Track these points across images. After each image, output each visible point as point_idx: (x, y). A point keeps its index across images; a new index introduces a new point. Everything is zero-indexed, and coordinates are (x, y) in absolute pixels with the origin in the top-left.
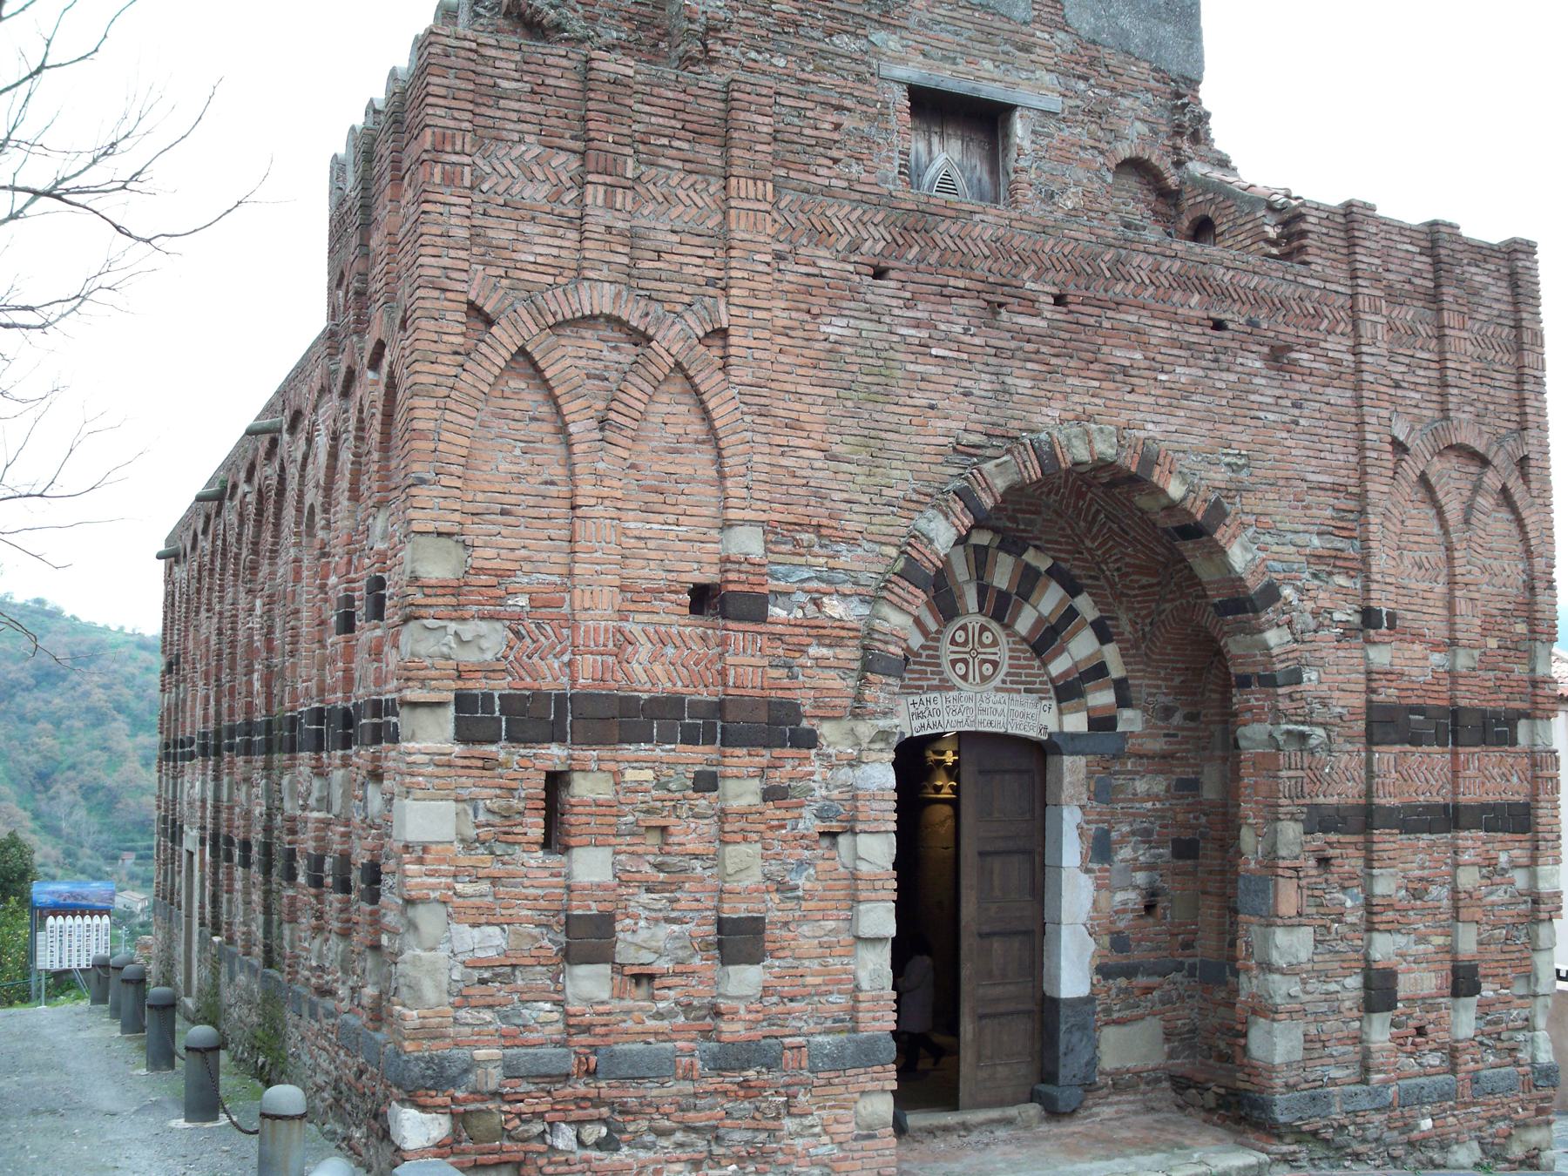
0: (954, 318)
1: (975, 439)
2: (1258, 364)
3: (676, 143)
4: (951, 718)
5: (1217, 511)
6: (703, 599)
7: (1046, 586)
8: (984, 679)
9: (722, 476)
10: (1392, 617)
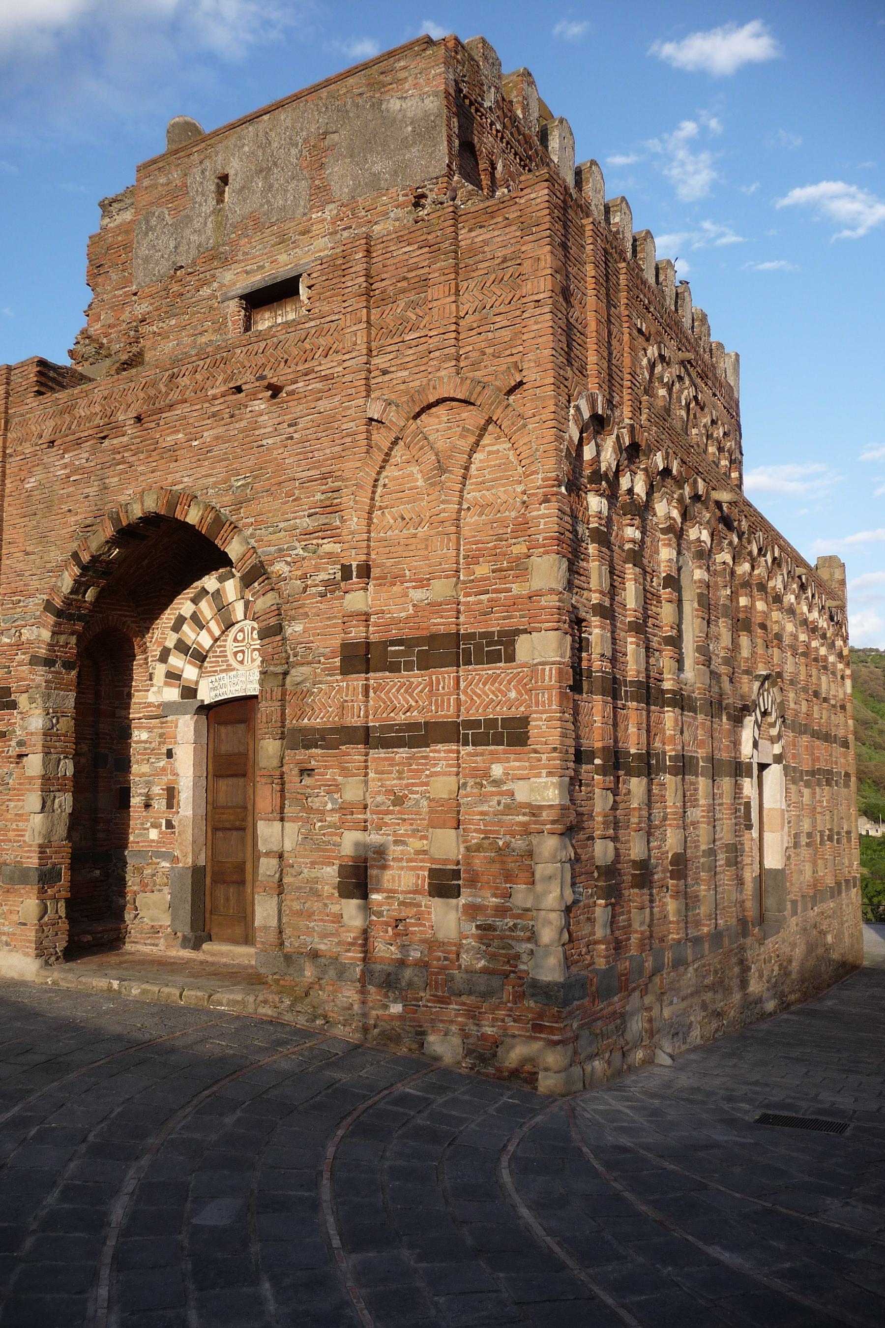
4: (233, 689)
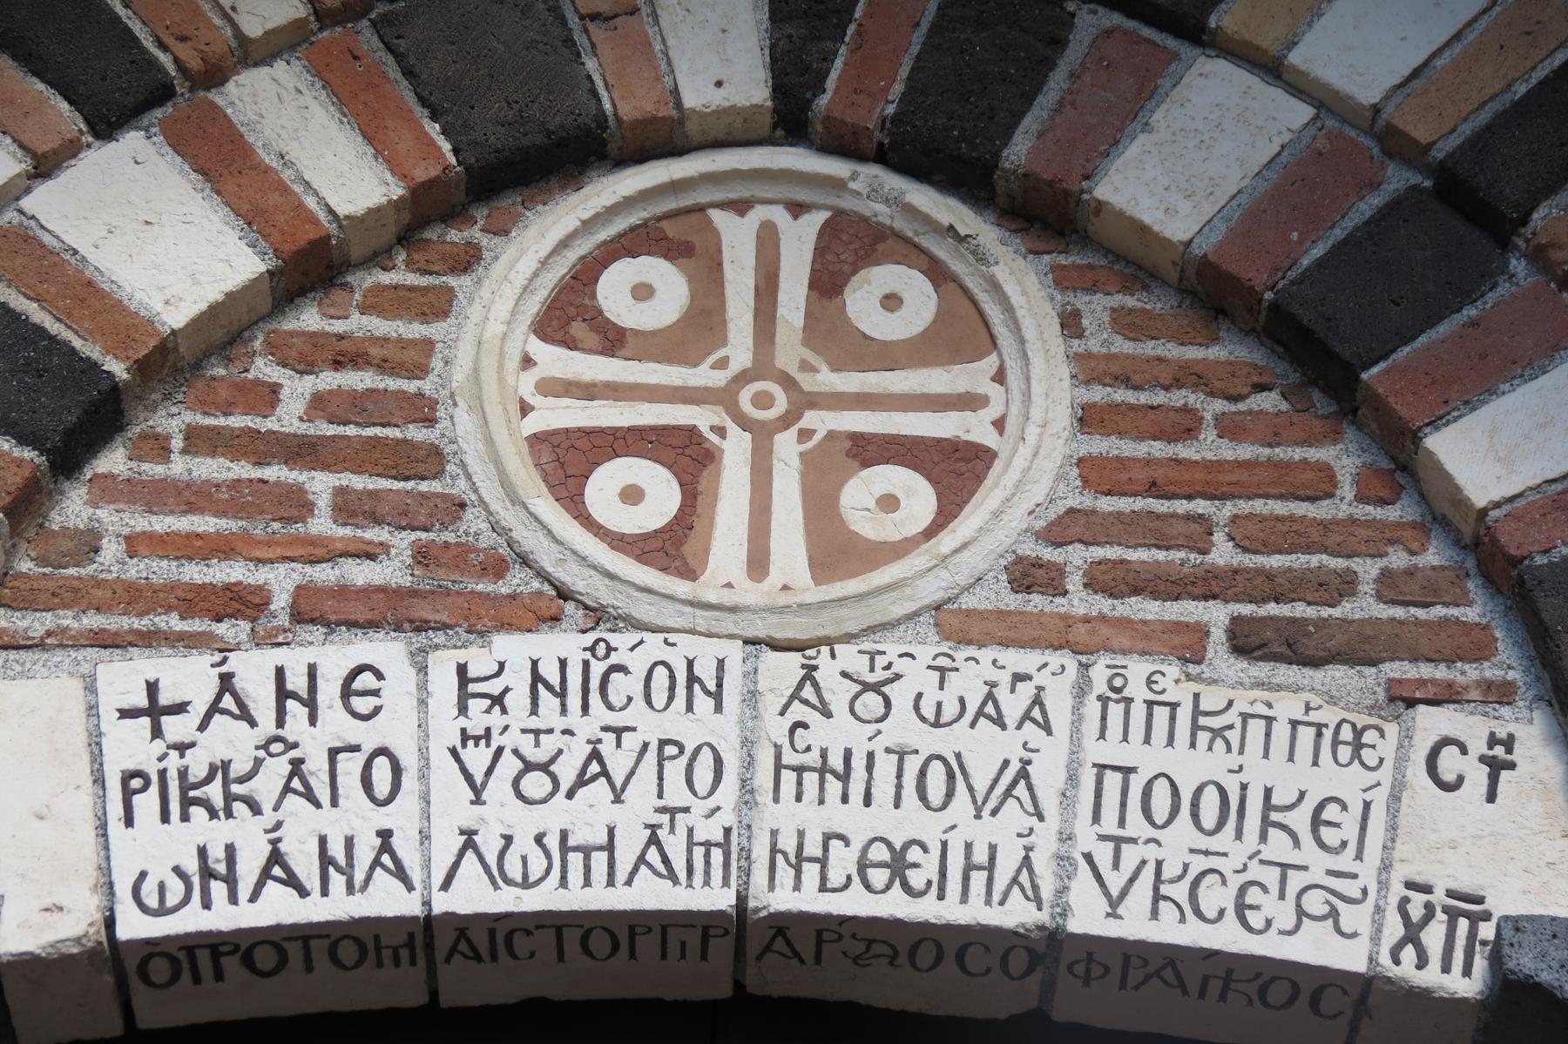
4: (500, 813)
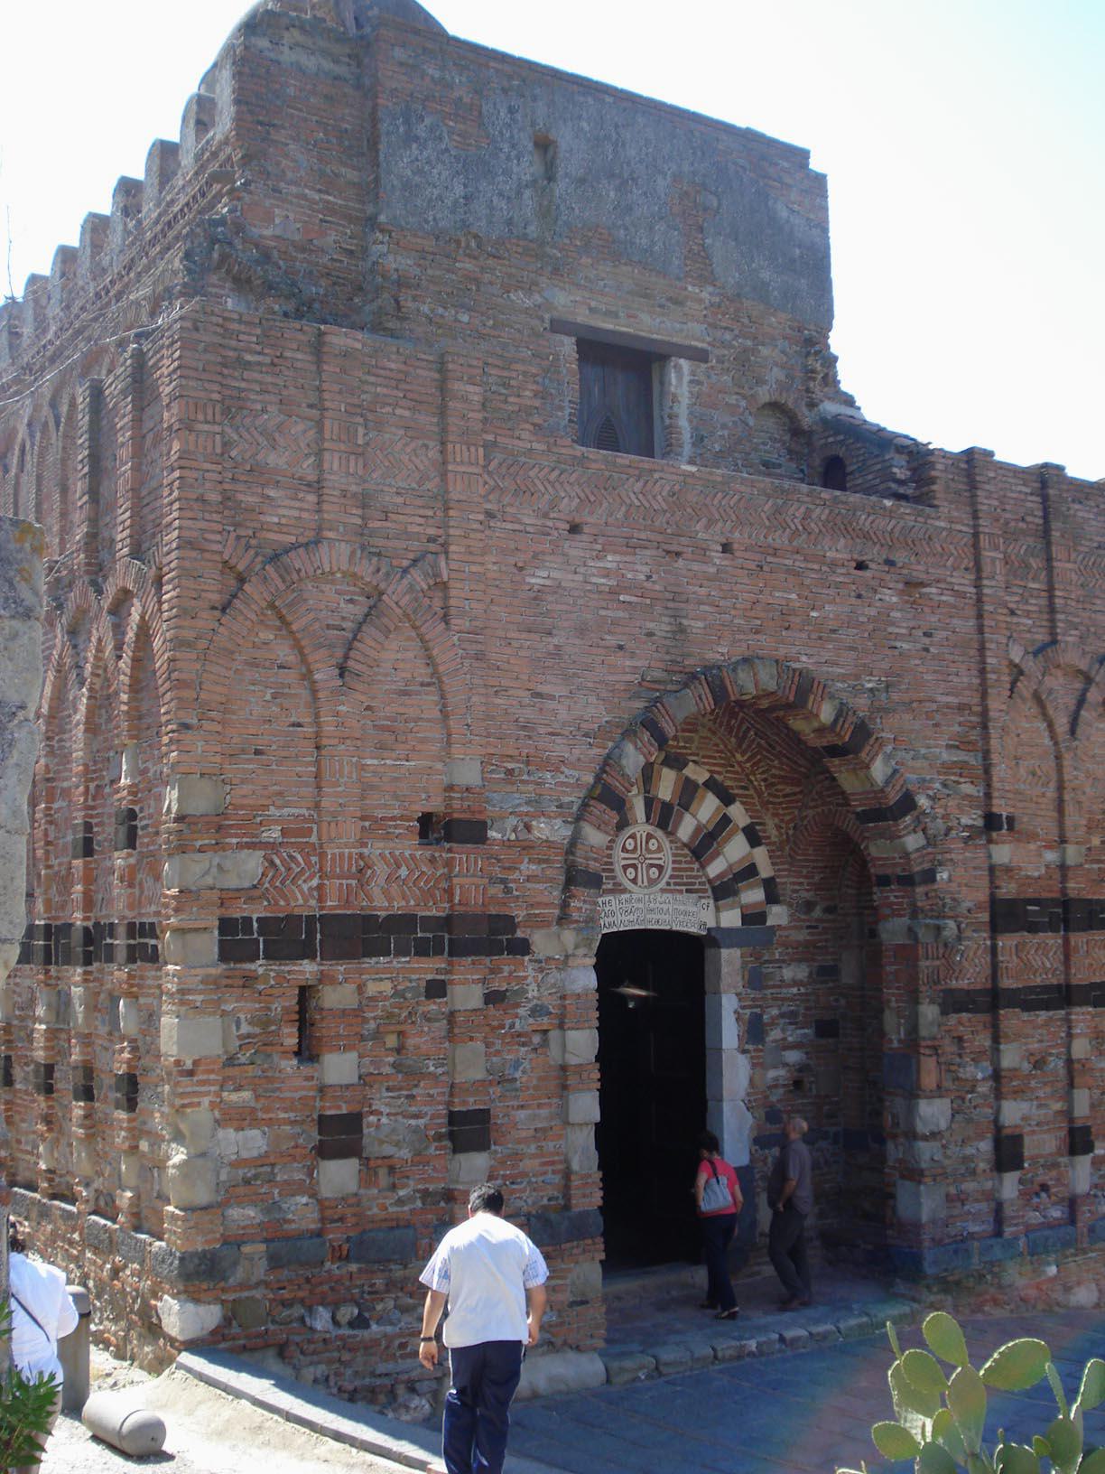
0: (638, 567)
1: (658, 674)
2: (894, 599)
3: (398, 411)
5: (863, 732)
6: (430, 827)
7: (703, 797)
8: (652, 882)
9: (445, 715)
10: (1011, 820)
